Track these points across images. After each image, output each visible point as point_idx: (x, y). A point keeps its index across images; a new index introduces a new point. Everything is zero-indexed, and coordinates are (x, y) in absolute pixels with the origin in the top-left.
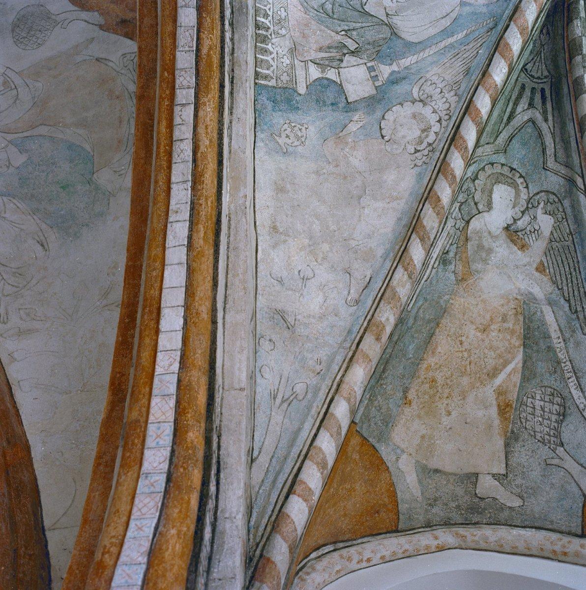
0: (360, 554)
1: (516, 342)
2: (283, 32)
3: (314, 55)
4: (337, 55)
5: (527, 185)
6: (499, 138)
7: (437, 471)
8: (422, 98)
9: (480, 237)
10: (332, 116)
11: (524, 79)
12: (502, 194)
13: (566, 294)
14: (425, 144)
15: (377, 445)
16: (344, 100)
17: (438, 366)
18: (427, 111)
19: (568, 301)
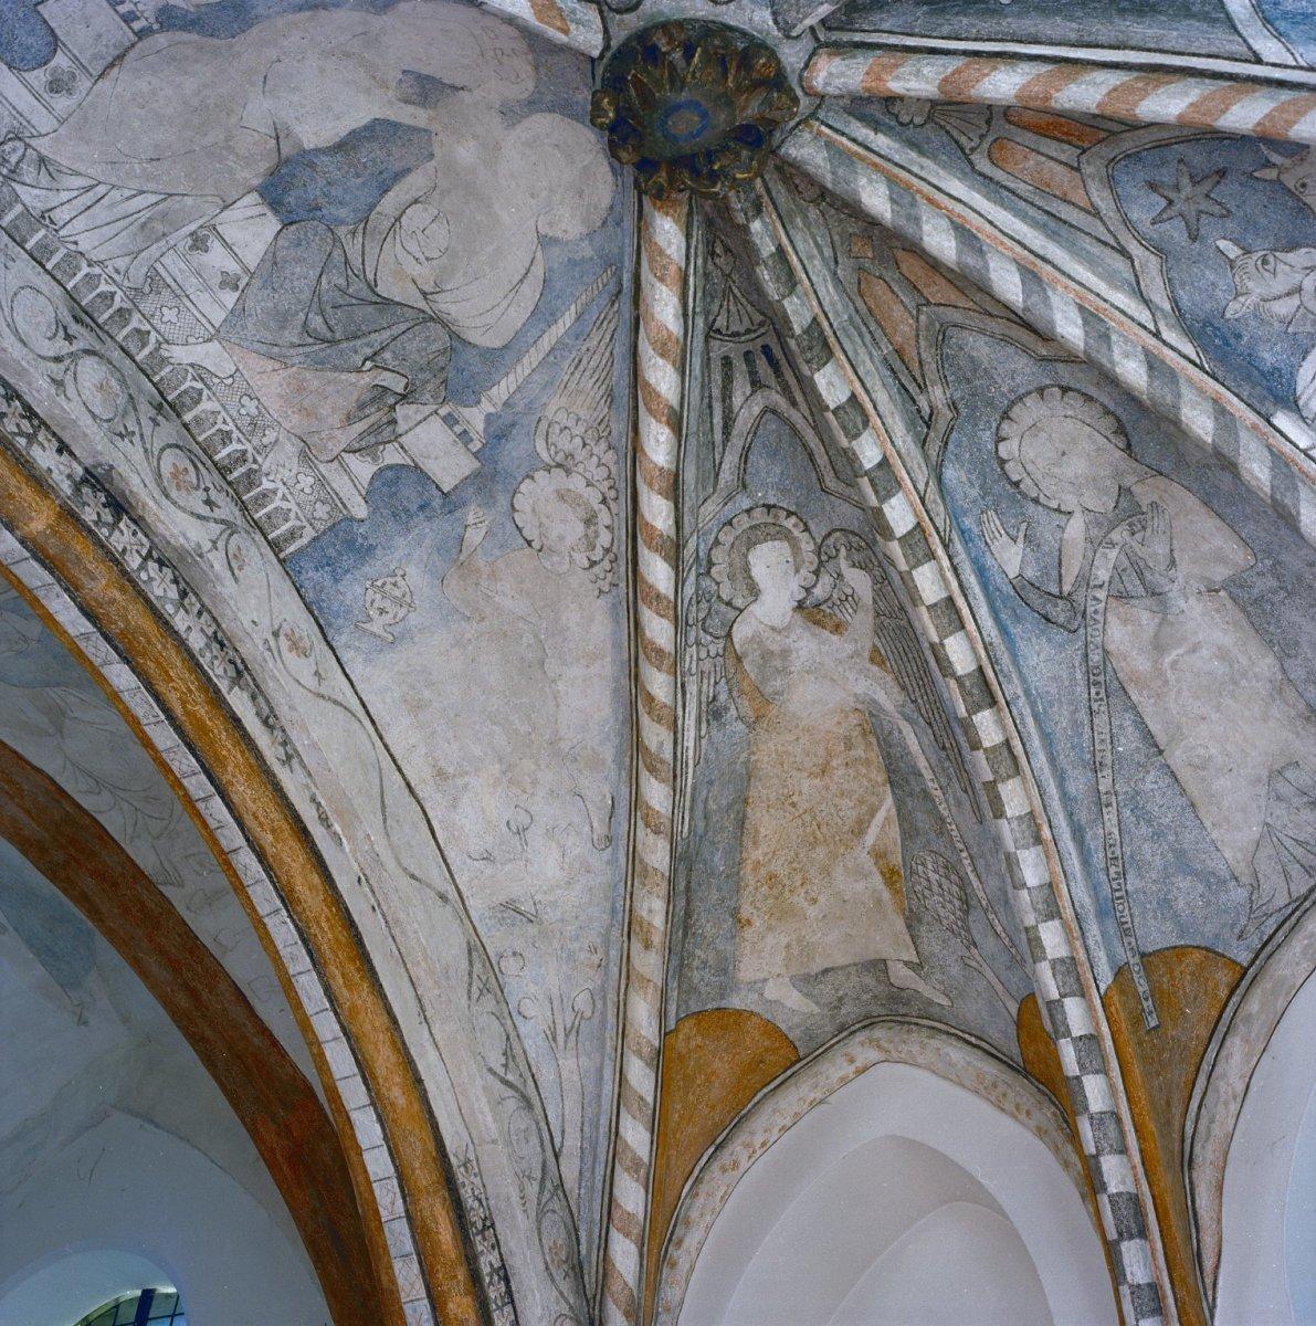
0: (747, 1146)
1: (881, 778)
2: (270, 436)
3: (345, 438)
4: (379, 416)
5: (805, 524)
6: (722, 475)
7: (826, 971)
8: (558, 459)
9: (760, 643)
10: (429, 531)
11: (719, 349)
12: (768, 561)
13: (923, 711)
14: (597, 554)
15: (723, 1004)
16: (435, 492)
17: (770, 856)
18: (576, 483)
19: (930, 724)
